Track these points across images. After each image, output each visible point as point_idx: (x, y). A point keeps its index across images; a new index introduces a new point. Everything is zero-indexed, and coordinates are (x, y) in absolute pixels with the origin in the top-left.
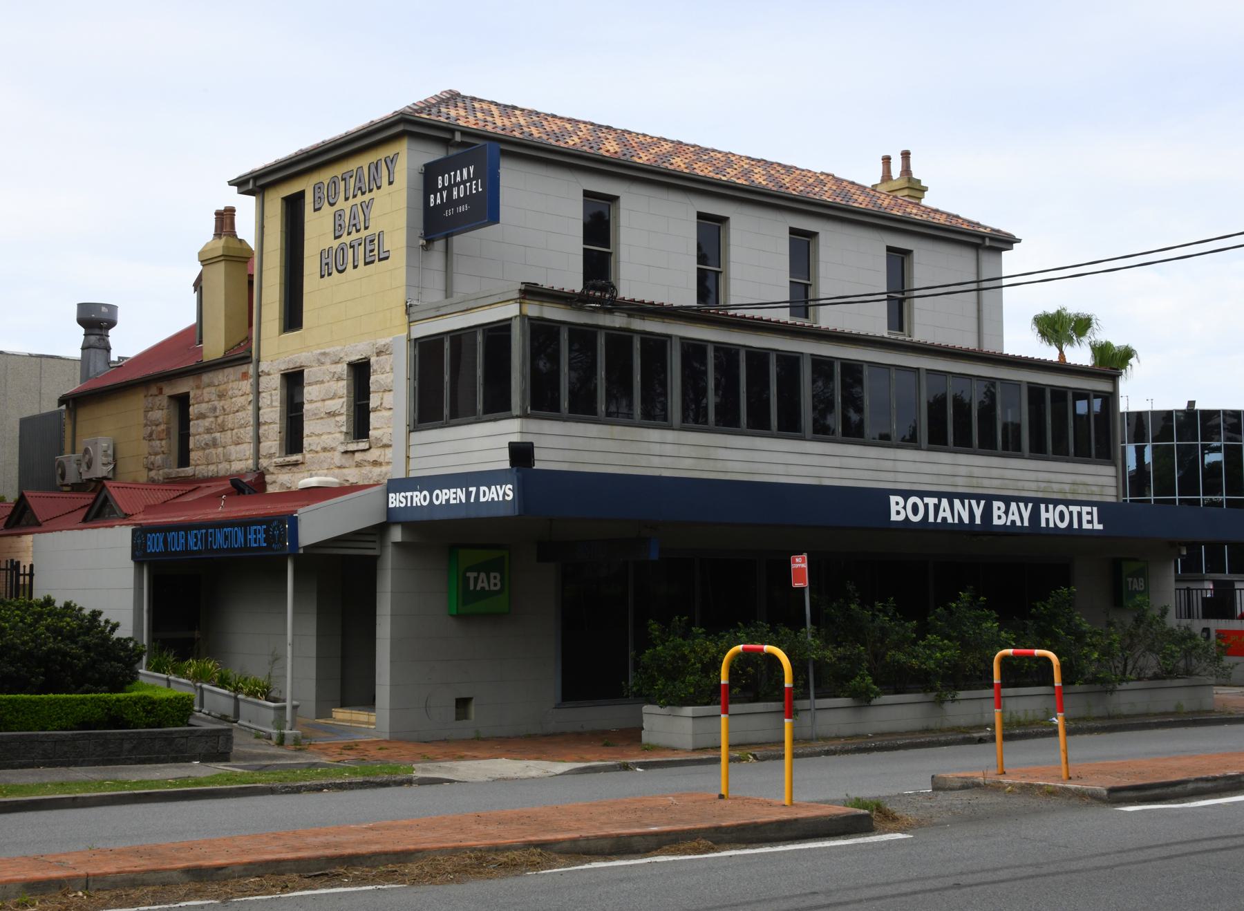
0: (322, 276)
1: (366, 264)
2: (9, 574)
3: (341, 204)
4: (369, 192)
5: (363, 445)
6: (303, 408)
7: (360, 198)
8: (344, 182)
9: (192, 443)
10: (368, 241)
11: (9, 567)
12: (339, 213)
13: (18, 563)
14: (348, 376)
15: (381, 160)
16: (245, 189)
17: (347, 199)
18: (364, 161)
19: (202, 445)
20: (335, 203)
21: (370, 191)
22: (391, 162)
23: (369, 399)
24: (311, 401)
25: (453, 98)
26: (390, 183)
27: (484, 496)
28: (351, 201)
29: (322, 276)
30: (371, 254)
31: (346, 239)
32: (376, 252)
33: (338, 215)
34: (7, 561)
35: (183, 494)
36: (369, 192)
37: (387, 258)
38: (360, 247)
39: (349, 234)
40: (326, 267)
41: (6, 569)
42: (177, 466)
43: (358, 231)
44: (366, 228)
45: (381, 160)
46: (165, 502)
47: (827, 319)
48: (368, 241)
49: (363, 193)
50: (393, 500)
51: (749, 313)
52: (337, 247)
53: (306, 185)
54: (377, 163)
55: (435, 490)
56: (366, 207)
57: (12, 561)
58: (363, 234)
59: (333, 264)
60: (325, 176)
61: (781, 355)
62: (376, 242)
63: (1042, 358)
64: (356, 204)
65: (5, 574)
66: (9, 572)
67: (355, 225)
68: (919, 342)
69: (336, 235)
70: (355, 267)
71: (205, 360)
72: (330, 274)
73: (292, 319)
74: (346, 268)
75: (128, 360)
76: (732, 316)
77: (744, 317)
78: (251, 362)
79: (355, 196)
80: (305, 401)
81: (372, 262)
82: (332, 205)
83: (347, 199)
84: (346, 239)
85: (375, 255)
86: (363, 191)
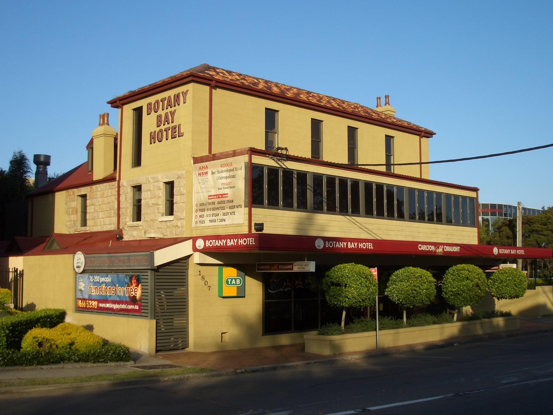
0: (151, 143)
1: (172, 138)
2: (13, 274)
3: (160, 112)
4: (174, 107)
5: (171, 218)
6: (141, 202)
7: (169, 109)
8: (162, 102)
9: (88, 216)
10: (173, 128)
11: (13, 271)
12: (159, 116)
13: (17, 269)
14: (163, 188)
15: (180, 93)
16: (115, 104)
17: (163, 110)
18: (171, 93)
19: (93, 217)
20: (157, 112)
21: (175, 106)
22: (185, 94)
23: (173, 198)
24: (145, 199)
25: (209, 68)
26: (184, 103)
27: (446, 249)
28: (165, 111)
29: (151, 143)
30: (175, 134)
31: (162, 127)
32: (177, 133)
33: (159, 117)
34: (12, 268)
35: (86, 239)
36: (174, 107)
37: (182, 136)
38: (169, 131)
39: (164, 125)
40: (153, 139)
41: (12, 272)
42: (80, 226)
43: (168, 124)
44: (172, 122)
45: (180, 93)
46: (78, 243)
47: (397, 170)
48: (173, 128)
49: (171, 107)
50: (208, 243)
51: (363, 167)
52: (158, 131)
53: (143, 103)
54: (178, 94)
55: (419, 245)
56: (173, 114)
57: (15, 268)
58: (171, 125)
59: (155, 138)
60: (152, 99)
61: (367, 183)
62: (177, 129)
63: (466, 186)
64: (168, 112)
65: (12, 274)
66: (13, 273)
67: (167, 121)
68: (423, 179)
69: (158, 126)
70: (167, 139)
71: (94, 180)
72: (154, 143)
73: (137, 161)
74: (162, 140)
75: (54, 179)
76: (360, 168)
77: (364, 168)
78: (116, 181)
79: (167, 109)
80: (142, 198)
81: (175, 137)
82: (156, 112)
83: (163, 110)
84: (162, 127)
85: (176, 134)
86: (171, 106)
